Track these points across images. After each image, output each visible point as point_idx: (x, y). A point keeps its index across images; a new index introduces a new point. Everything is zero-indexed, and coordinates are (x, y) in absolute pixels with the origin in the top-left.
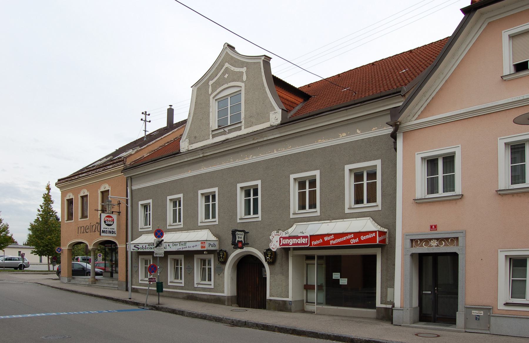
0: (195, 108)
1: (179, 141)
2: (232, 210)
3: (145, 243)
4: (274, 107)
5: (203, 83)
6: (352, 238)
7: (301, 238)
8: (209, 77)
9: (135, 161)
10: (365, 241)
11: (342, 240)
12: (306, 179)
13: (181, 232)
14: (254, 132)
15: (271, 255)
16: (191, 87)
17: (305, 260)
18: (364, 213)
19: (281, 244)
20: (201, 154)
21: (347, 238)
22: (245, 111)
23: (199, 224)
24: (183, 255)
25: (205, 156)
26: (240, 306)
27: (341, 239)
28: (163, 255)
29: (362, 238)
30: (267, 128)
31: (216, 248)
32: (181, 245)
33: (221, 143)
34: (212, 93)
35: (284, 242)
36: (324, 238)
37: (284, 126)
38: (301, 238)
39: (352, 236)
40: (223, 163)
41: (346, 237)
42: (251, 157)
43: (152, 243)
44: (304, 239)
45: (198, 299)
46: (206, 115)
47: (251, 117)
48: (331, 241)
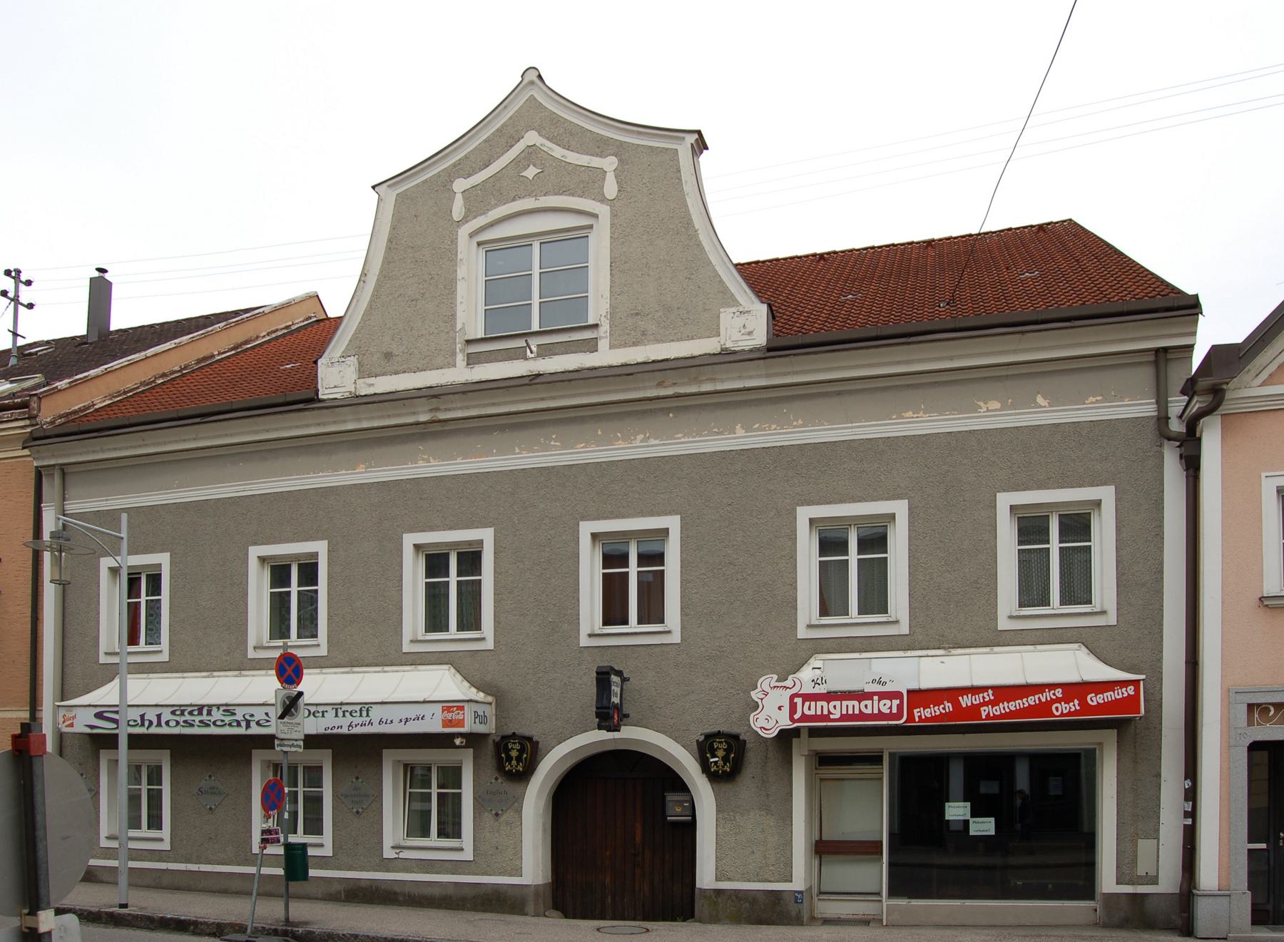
0: (385, 258)
1: (316, 362)
2: (555, 605)
3: (156, 706)
4: (733, 295)
5: (426, 181)
6: (1058, 700)
7: (876, 698)
8: (454, 165)
9: (67, 415)
10: (1100, 708)
11: (1023, 704)
12: (850, 525)
13: (318, 671)
14: (653, 362)
15: (728, 751)
16: (374, 187)
17: (816, 769)
18: (1060, 631)
19: (797, 716)
20: (425, 412)
21: (1039, 698)
22: (611, 292)
23: (407, 647)
24: (331, 750)
25: (440, 421)
26: (566, 917)
27: (1020, 701)
28: (300, 747)
29: (1093, 701)
30: (705, 354)
31: (489, 728)
32: (344, 716)
33: (526, 381)
34: (465, 220)
35: (809, 709)
36: (960, 698)
37: (795, 355)
38: (876, 698)
39: (1059, 692)
40: (517, 451)
41: (1037, 696)
42: (641, 442)
43: (191, 705)
44: (888, 702)
45: (401, 898)
46: (441, 286)
47: (637, 314)
48: (986, 708)
